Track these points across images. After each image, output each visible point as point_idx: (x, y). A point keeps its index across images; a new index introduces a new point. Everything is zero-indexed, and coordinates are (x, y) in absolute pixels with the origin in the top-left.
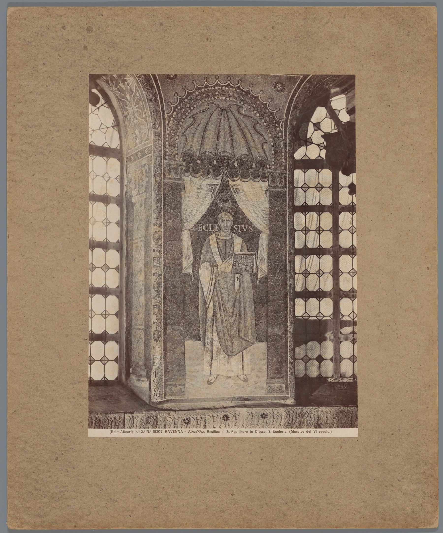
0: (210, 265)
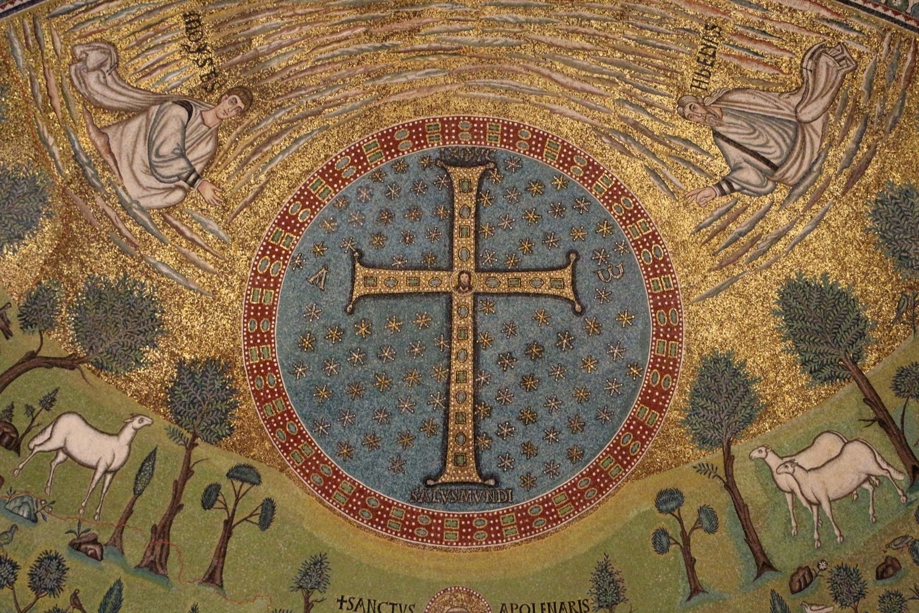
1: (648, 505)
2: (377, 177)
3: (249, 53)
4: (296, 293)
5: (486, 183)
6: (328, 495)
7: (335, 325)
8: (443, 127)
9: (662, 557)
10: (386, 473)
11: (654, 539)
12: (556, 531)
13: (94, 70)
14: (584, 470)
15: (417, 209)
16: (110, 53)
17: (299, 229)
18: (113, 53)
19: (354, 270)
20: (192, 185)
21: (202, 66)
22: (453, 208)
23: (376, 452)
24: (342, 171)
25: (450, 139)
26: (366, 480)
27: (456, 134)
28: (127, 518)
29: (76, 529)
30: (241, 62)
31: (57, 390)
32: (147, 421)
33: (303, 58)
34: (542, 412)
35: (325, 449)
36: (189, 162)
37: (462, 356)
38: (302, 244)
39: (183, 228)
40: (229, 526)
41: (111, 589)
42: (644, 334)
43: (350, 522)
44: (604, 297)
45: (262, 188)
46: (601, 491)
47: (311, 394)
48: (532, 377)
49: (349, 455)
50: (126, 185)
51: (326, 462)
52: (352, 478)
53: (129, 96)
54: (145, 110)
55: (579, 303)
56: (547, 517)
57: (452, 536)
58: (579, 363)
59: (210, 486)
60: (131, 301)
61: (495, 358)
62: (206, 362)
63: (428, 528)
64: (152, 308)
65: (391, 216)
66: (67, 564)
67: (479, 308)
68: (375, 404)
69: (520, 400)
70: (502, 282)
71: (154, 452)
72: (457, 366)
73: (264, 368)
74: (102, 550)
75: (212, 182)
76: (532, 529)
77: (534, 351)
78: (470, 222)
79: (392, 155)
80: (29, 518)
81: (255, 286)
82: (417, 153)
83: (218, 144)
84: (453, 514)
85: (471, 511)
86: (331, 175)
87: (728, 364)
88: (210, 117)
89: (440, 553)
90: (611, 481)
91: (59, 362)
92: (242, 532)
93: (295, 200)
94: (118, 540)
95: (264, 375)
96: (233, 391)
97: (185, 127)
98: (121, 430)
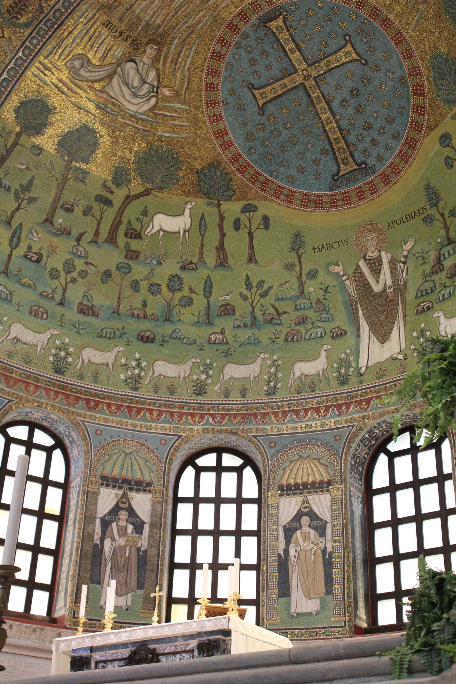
0: (112, 540)
1: (437, 147)
2: (238, 46)
3: (143, 23)
4: (233, 117)
5: (288, 23)
6: (291, 203)
7: (258, 123)
8: (252, 7)
9: (451, 170)
10: (314, 182)
11: (445, 162)
12: (401, 177)
13: (81, 68)
14: (403, 141)
15: (265, 51)
16: (83, 58)
17: (217, 88)
18: (84, 57)
19: (253, 94)
20: (157, 92)
21: (126, 40)
22: (280, 42)
23: (305, 173)
24: (220, 51)
25: (259, 11)
26: (306, 188)
27: (260, 7)
28: (202, 248)
29: (180, 261)
30: (142, 29)
31: (146, 207)
32: (194, 203)
33: (168, 12)
34: (372, 121)
35: (281, 182)
36: (149, 84)
37: (323, 111)
38: (222, 94)
39: (165, 113)
40: (250, 234)
41: (206, 280)
42: (398, 60)
43: (306, 211)
44: (371, 50)
45: (189, 78)
46: (414, 148)
47: (263, 159)
48: (360, 106)
49: (293, 180)
50: (128, 107)
51: (284, 188)
52: (300, 190)
53: (104, 70)
54: (115, 72)
55: (363, 59)
56: (394, 172)
57: (355, 199)
58: (378, 89)
59: (235, 220)
60: (160, 155)
61: (339, 105)
62: (208, 166)
63: (342, 199)
64: (171, 154)
65: (255, 61)
66: (182, 277)
67: (319, 84)
68: (295, 151)
69: (360, 121)
70: (323, 67)
71: (203, 215)
72: (324, 117)
73: (236, 158)
74: (196, 266)
75: (165, 87)
76: (390, 181)
77: (355, 93)
78: (292, 45)
79: (237, 32)
80: (157, 264)
81: (213, 123)
82: (248, 25)
83: (157, 70)
84: (350, 188)
85: (360, 184)
86: (216, 56)
87: (441, 57)
88: (145, 60)
89: (352, 210)
90: (417, 142)
91: (141, 195)
92: (257, 235)
93: (207, 76)
94: (202, 260)
95: (237, 160)
96: (227, 174)
97: (138, 70)
98: (184, 211)
